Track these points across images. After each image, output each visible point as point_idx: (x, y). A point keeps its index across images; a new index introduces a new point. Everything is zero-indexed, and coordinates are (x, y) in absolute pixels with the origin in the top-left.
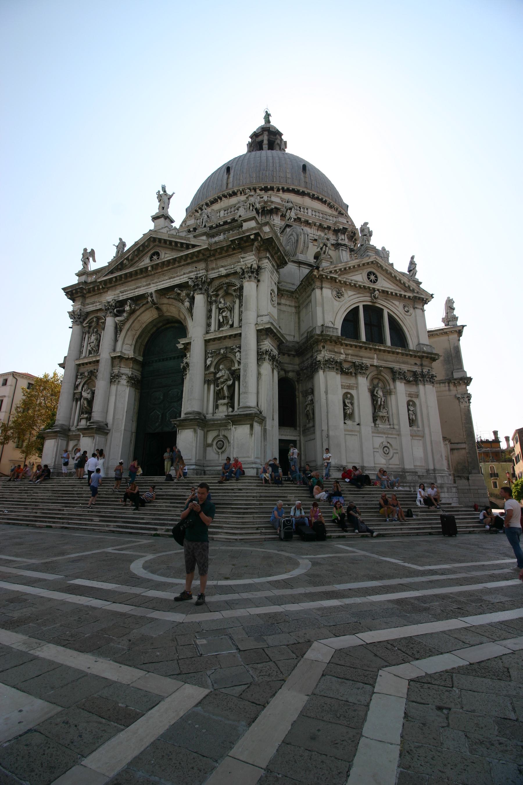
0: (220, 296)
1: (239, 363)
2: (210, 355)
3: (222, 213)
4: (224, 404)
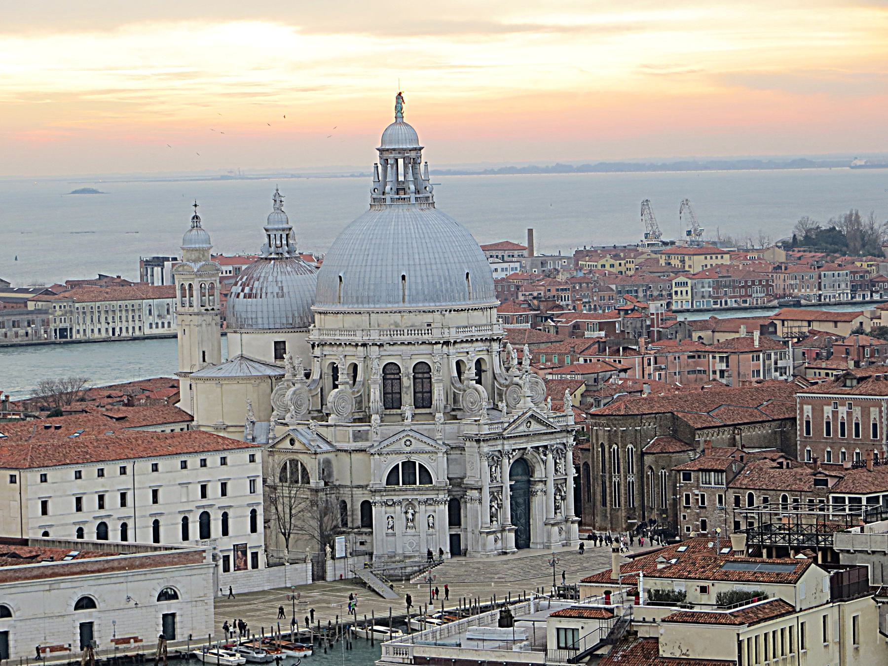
3: (473, 328)
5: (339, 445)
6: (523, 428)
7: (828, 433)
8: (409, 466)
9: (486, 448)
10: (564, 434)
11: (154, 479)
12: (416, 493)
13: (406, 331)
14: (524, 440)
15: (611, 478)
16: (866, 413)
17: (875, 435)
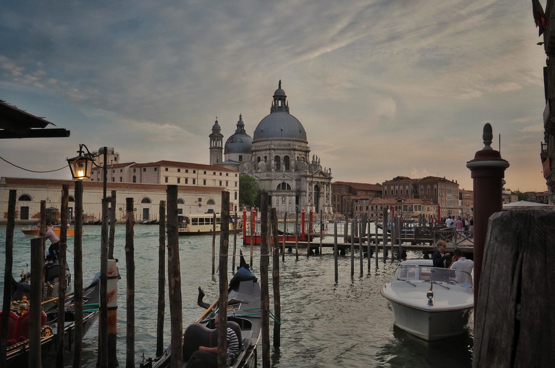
5: (261, 178)
6: (318, 175)
7: (392, 194)
8: (284, 184)
9: (308, 179)
11: (205, 177)
16: (404, 187)
17: (407, 193)
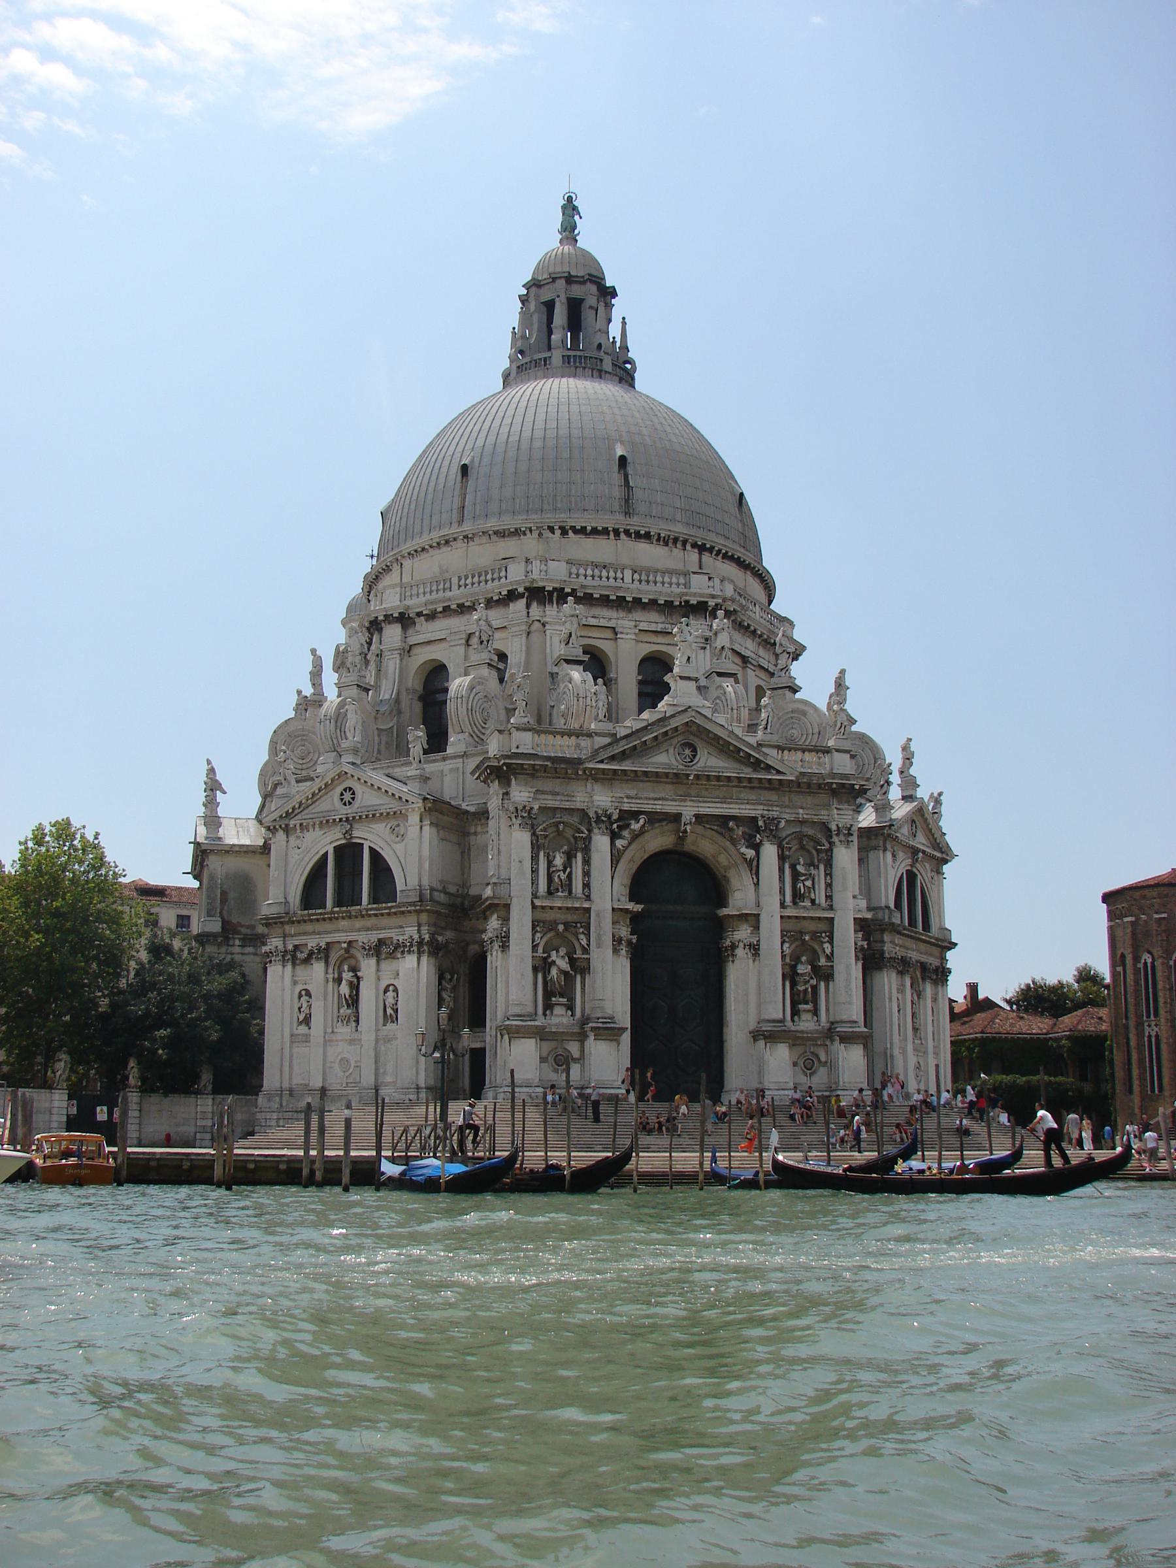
0: (793, 849)
1: (830, 958)
2: (787, 940)
4: (809, 1011)
9: (521, 794)
10: (823, 797)
12: (359, 923)
13: (455, 581)
14: (667, 790)
15: (1139, 1025)
